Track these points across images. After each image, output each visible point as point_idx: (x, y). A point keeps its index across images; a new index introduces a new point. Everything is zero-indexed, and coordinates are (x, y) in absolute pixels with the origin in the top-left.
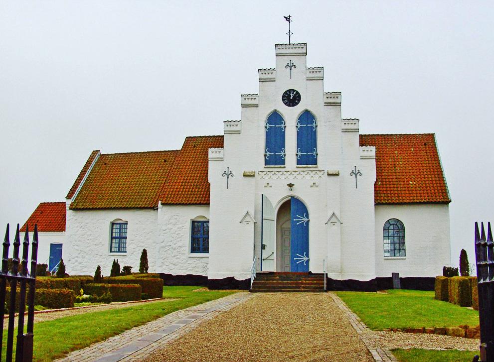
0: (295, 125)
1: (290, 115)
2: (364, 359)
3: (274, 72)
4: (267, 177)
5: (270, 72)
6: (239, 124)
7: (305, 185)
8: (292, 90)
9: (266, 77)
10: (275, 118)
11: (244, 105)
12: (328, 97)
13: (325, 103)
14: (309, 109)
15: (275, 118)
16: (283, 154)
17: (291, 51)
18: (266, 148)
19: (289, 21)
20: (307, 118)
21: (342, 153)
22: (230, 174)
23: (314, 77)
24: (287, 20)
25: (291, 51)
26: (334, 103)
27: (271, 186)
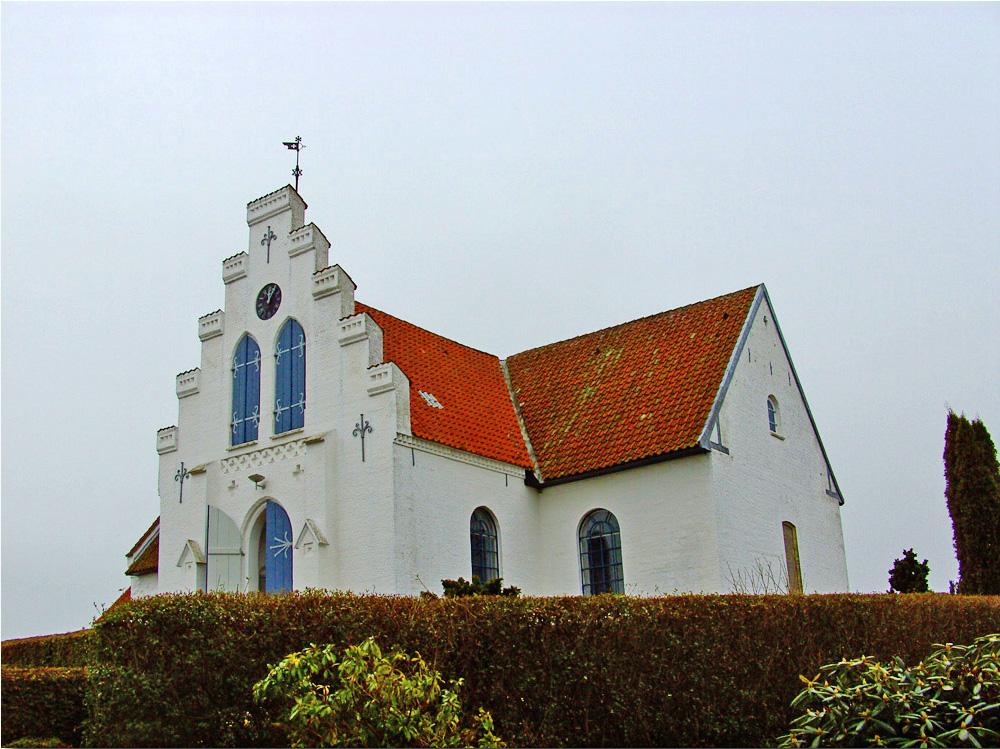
0: (274, 352)
1: (266, 335)
2: (924, 745)
3: (243, 260)
4: (232, 470)
5: (232, 263)
6: (194, 375)
7: (289, 475)
8: (262, 290)
9: (234, 271)
10: (247, 347)
11: (206, 335)
12: (318, 282)
13: (314, 295)
14: (249, 331)
15: (247, 347)
16: (255, 417)
17: (282, 210)
18: (277, 399)
19: (297, 148)
20: (292, 332)
21: (341, 391)
22: (367, 427)
23: (300, 248)
24: (290, 148)
25: (282, 210)
26: (327, 290)
27: (233, 482)
